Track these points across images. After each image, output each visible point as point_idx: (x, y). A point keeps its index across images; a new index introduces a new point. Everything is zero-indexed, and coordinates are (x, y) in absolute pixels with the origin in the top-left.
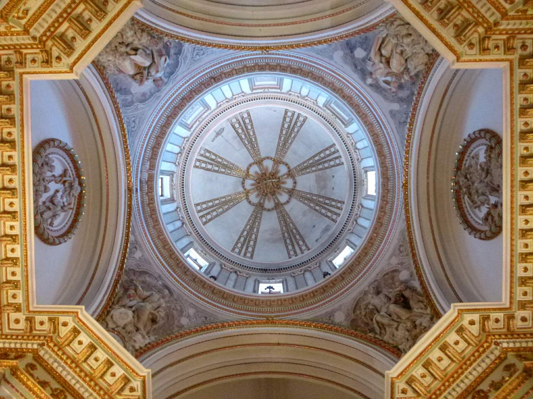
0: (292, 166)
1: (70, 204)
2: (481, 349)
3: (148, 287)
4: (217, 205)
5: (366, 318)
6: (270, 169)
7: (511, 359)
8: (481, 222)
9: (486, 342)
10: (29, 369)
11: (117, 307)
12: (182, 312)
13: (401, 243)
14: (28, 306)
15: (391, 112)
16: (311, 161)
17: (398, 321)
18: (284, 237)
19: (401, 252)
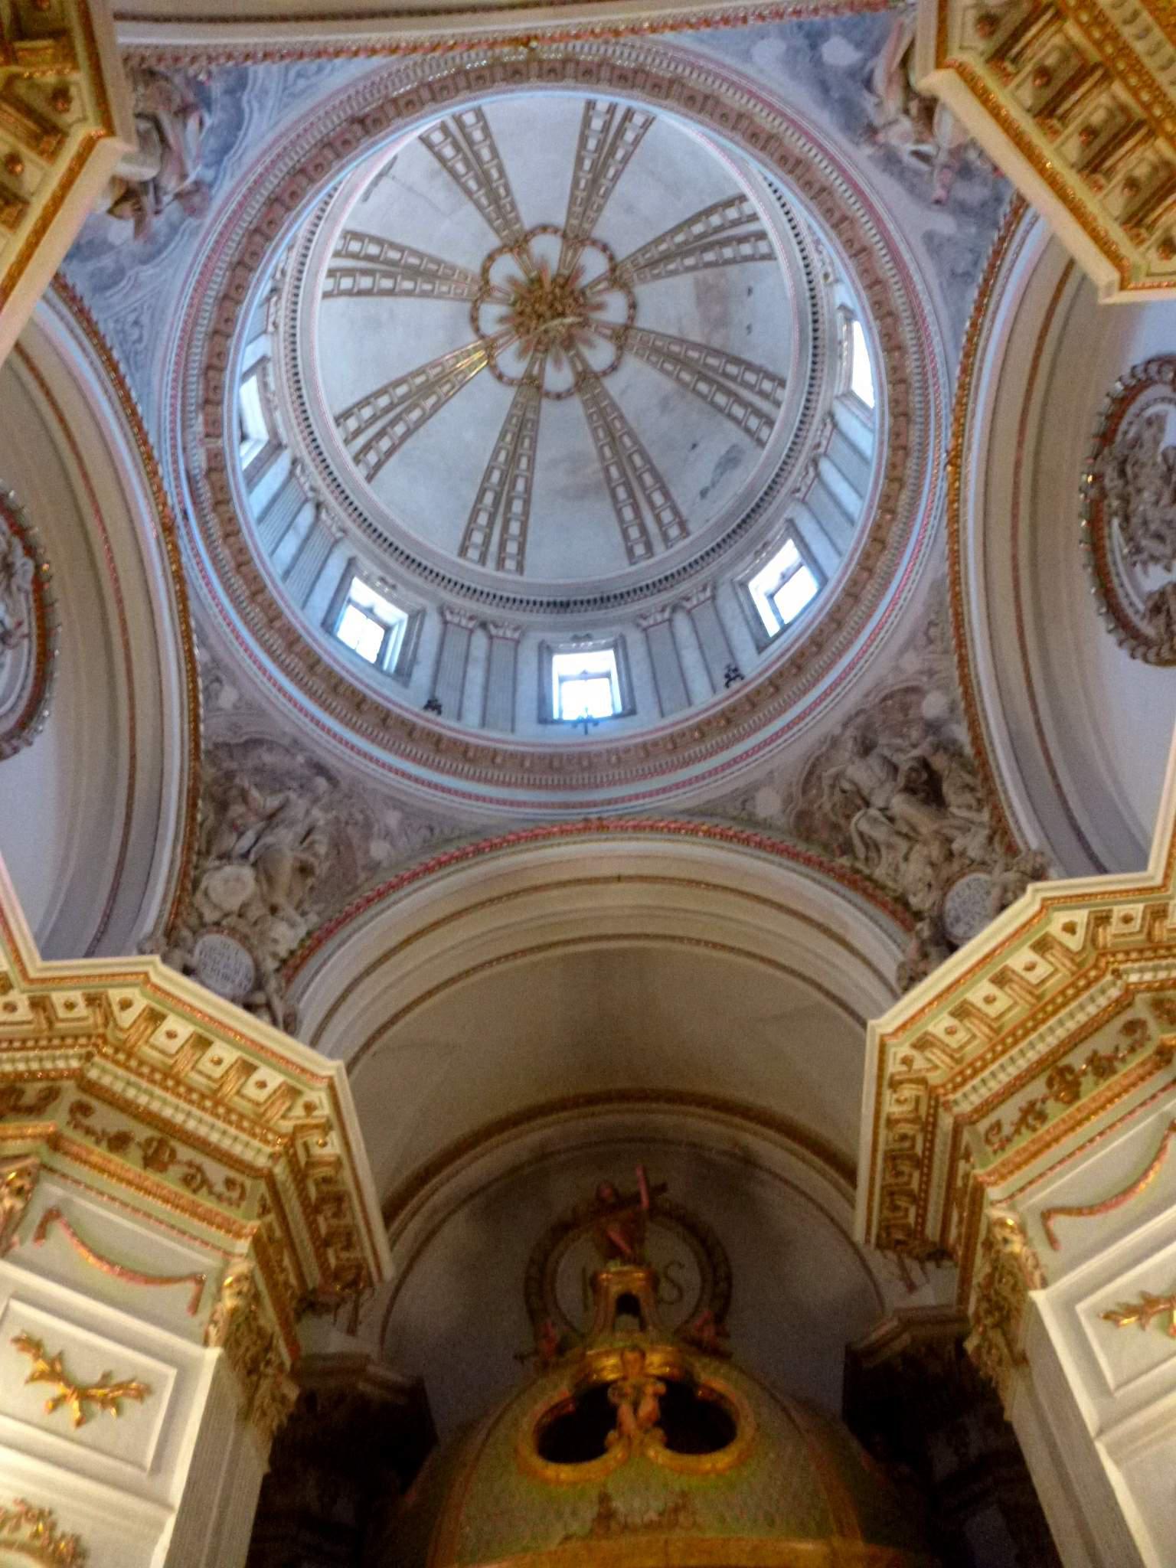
0: (622, 252)
1: (19, 624)
2: (1082, 983)
3: (274, 780)
4: (403, 398)
5: (836, 815)
6: (553, 266)
7: (1141, 1010)
8: (1141, 607)
9: (1095, 966)
10: (79, 1116)
11: (211, 862)
12: (368, 825)
13: (933, 617)
14: (24, 972)
15: (929, 237)
16: (680, 238)
17: (911, 836)
18: (608, 478)
19: (930, 641)
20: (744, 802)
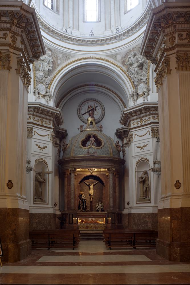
12: (57, 58)
20: (116, 56)
